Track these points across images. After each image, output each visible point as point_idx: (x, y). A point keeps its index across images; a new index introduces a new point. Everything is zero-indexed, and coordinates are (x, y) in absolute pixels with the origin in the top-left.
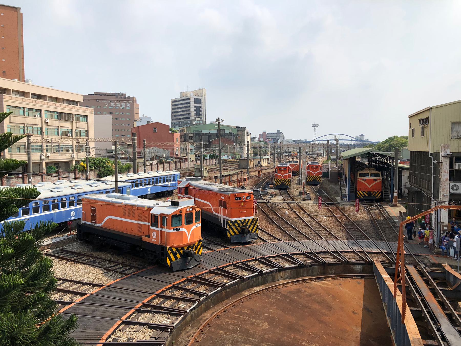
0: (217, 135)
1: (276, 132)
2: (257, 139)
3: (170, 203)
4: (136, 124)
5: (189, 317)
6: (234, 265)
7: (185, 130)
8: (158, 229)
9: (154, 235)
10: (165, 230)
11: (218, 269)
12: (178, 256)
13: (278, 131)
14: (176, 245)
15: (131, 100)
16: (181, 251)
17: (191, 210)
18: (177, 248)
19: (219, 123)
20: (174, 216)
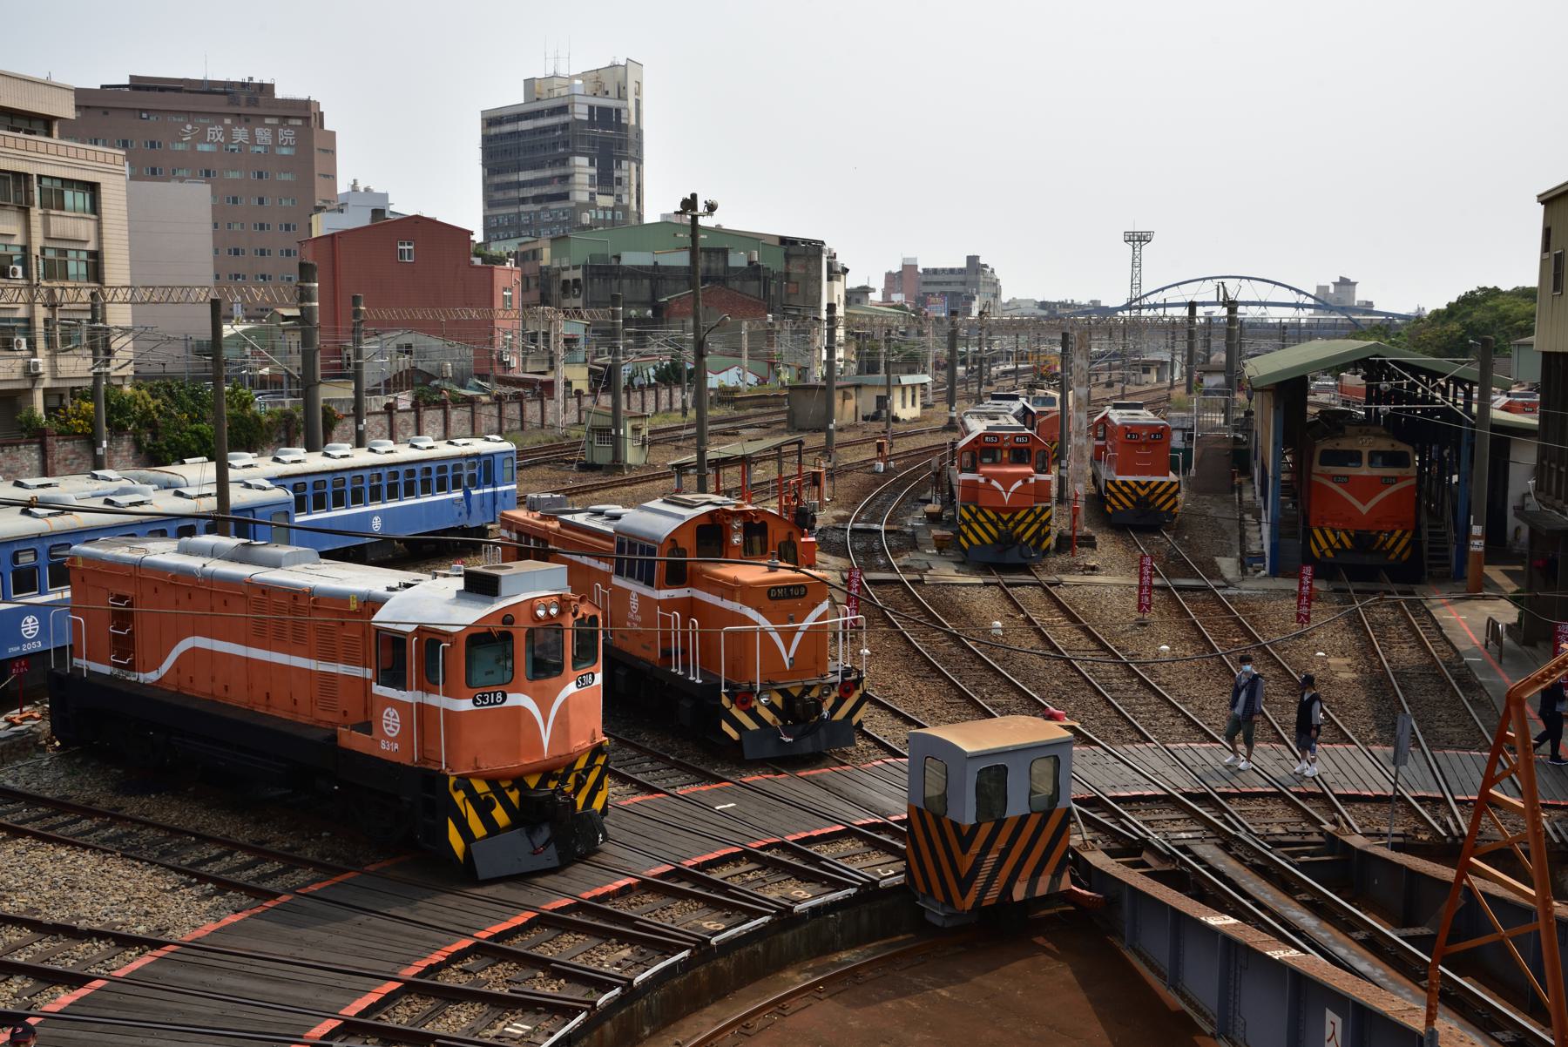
0: (689, 275)
1: (962, 264)
2: (876, 297)
3: (460, 583)
4: (322, 225)
6: (749, 855)
7: (546, 252)
8: (409, 697)
9: (391, 722)
10: (438, 701)
11: (679, 874)
12: (500, 815)
13: (972, 260)
14: (490, 764)
15: (304, 114)
16: (514, 796)
17: (553, 611)
18: (493, 781)
19: (694, 218)
20: (478, 639)
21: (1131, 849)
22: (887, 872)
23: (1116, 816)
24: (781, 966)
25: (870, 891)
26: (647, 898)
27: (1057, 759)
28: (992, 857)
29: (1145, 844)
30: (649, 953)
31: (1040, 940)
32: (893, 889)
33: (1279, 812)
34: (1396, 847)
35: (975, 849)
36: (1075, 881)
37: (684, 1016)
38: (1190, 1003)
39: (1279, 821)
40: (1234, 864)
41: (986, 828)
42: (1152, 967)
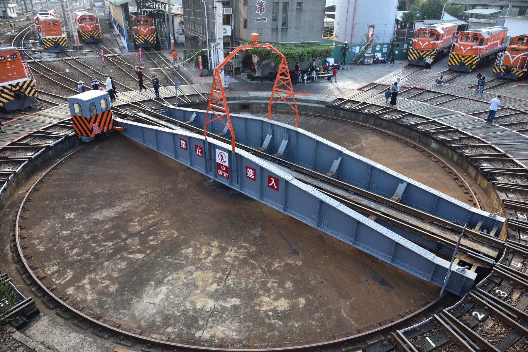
22: (70, 133)
23: (118, 110)
25: (67, 137)
32: (73, 136)
34: (178, 106)
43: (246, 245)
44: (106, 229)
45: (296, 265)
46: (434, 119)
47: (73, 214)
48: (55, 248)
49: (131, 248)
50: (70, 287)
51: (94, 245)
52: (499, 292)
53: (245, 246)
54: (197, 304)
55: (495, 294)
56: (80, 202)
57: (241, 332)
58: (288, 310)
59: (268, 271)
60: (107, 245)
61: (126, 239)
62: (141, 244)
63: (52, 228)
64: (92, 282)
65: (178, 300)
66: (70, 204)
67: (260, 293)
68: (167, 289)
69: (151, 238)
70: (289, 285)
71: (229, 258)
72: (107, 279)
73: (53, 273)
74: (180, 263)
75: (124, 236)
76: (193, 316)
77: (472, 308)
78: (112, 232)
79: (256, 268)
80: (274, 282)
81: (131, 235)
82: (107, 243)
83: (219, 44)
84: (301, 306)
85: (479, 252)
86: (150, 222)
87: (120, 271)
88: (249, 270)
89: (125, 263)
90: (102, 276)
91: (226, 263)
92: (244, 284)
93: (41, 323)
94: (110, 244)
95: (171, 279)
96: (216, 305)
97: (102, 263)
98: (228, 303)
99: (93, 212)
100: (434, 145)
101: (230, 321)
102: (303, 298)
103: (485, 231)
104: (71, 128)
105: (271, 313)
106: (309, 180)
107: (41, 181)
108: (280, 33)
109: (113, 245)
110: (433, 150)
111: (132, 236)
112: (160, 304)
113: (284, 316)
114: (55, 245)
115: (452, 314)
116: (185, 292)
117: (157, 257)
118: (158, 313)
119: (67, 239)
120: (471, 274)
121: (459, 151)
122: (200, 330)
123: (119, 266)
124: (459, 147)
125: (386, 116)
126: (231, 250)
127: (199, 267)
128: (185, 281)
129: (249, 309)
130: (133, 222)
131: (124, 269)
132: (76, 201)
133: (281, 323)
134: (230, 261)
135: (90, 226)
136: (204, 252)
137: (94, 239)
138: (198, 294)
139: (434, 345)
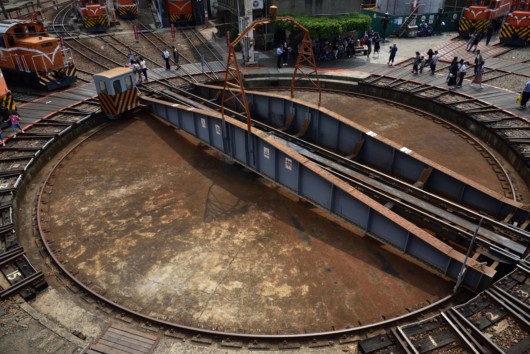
5: (29, 175)
21: (151, 94)
22: (97, 110)
23: (145, 87)
24: (77, 136)
25: (94, 115)
26: (37, 128)
27: (130, 76)
28: (121, 101)
29: (154, 92)
30: (44, 141)
31: (136, 118)
32: (99, 113)
33: (180, 81)
34: (205, 84)
35: (117, 100)
36: (141, 103)
37: (57, 153)
38: (172, 124)
39: (180, 82)
40: (173, 93)
41: (118, 95)
42: (162, 118)
43: (257, 227)
44: (121, 207)
45: (305, 251)
46: (476, 98)
47: (93, 190)
48: (72, 224)
49: (143, 226)
50: (81, 262)
51: (108, 222)
52: (520, 292)
53: (256, 229)
54: (199, 286)
55: (515, 295)
56: (100, 179)
57: (239, 316)
58: (290, 297)
59: (274, 256)
60: (120, 223)
61: (140, 217)
62: (153, 221)
63: (72, 203)
64: (103, 258)
65: (182, 280)
66: (91, 180)
67: (264, 277)
68: (173, 269)
69: (163, 217)
70: (294, 271)
71: (237, 240)
72: (117, 256)
73: (67, 249)
74: (188, 244)
75: (138, 214)
76: (194, 297)
77: (485, 308)
78: (127, 210)
79: (263, 252)
80: (279, 267)
81: (145, 214)
82: (121, 221)
83: (248, 18)
84: (303, 294)
85: (504, 247)
86: (165, 201)
87: (130, 248)
88: (255, 252)
89: (136, 241)
90: (113, 253)
91: (234, 245)
92: (248, 267)
93: (48, 296)
94: (124, 221)
95: (177, 258)
96: (218, 288)
97: (114, 240)
98: (230, 285)
99: (111, 189)
100: (472, 127)
101: (229, 304)
102: (306, 285)
103: (516, 224)
104: (98, 105)
105: (272, 299)
106: (327, 162)
107: (67, 158)
108: (314, 4)
109: (127, 222)
110: (471, 132)
111: (145, 215)
112: (164, 283)
113: (286, 303)
114: (72, 221)
115: (461, 312)
116: (190, 272)
117: (167, 236)
118: (160, 292)
119: (84, 215)
120: (491, 272)
121: (500, 134)
122: (199, 311)
123: (129, 244)
124: (500, 129)
125: (423, 94)
126: (241, 233)
127: (206, 248)
128: (191, 261)
129: (251, 293)
130: (148, 200)
131: (134, 247)
132: (97, 178)
133: (280, 309)
134: (238, 244)
135: (107, 204)
136: (213, 233)
137: (109, 216)
138: (202, 275)
139: (435, 344)
